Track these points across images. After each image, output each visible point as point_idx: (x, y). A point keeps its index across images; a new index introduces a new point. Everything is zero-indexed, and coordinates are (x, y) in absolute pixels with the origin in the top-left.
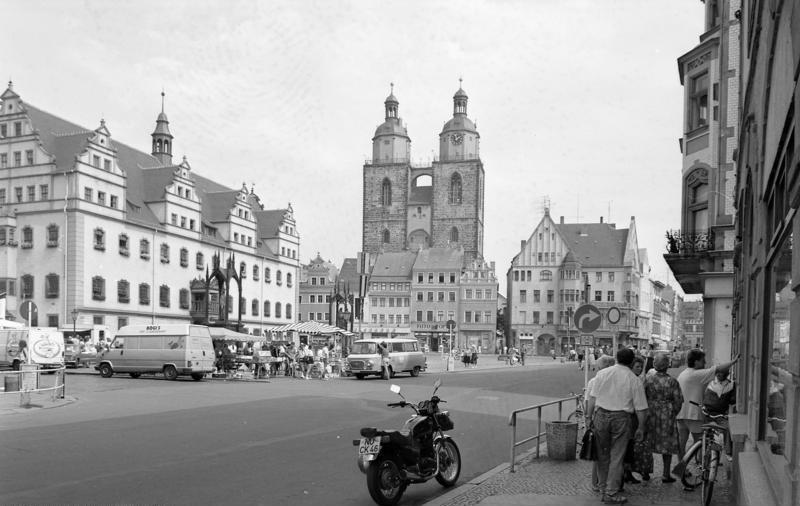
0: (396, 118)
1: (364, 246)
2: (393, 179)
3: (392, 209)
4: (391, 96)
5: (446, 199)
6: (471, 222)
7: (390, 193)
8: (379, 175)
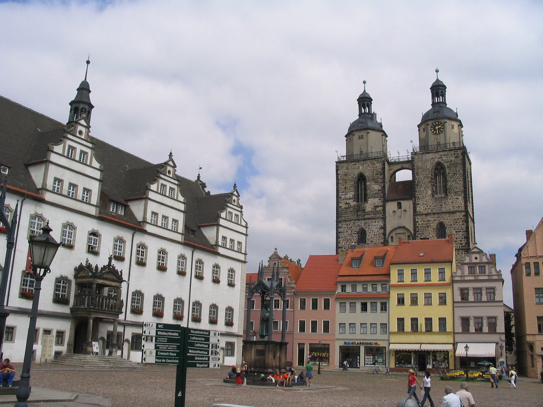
0: (370, 113)
1: (338, 247)
2: (367, 174)
3: (369, 206)
4: (365, 91)
5: (430, 192)
6: (461, 215)
7: (365, 190)
8: (356, 170)
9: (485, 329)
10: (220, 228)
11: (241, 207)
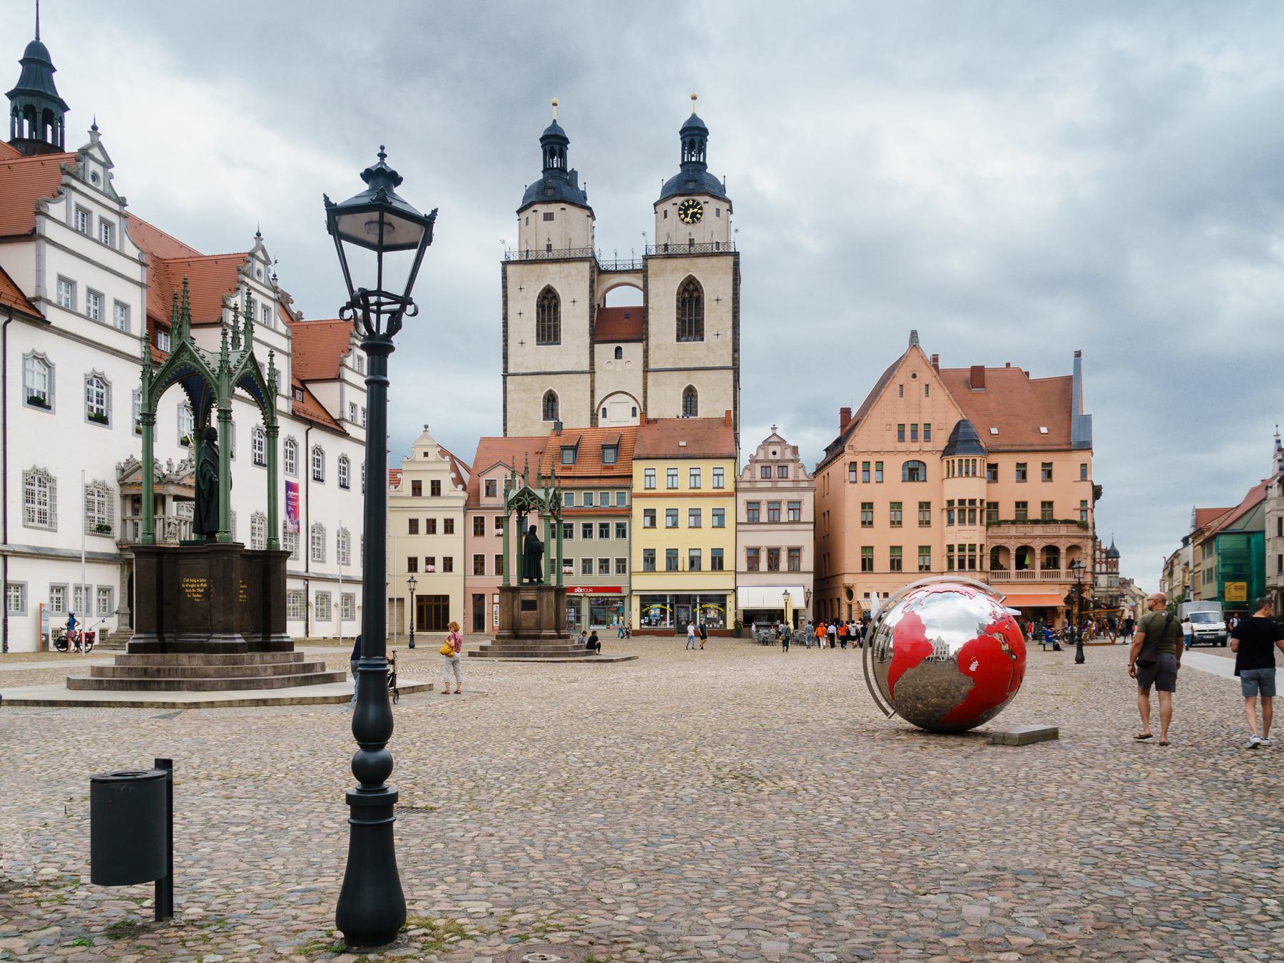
9: (763, 565)
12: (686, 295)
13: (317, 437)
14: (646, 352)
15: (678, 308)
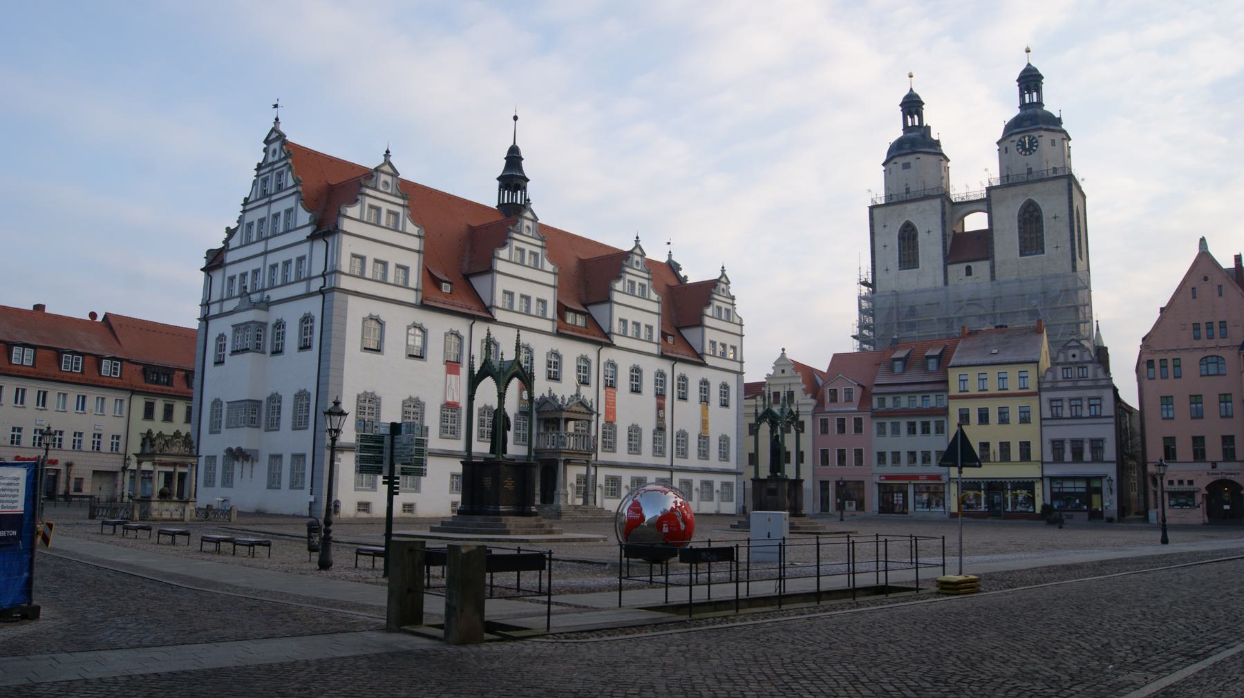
10: (707, 330)
11: (733, 298)
12: (1027, 215)
13: (681, 369)
14: (993, 268)
15: (1020, 228)
